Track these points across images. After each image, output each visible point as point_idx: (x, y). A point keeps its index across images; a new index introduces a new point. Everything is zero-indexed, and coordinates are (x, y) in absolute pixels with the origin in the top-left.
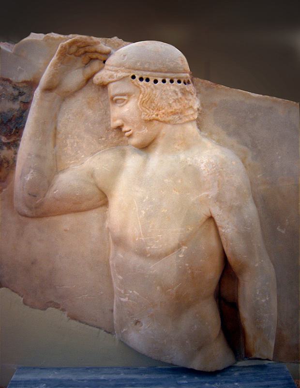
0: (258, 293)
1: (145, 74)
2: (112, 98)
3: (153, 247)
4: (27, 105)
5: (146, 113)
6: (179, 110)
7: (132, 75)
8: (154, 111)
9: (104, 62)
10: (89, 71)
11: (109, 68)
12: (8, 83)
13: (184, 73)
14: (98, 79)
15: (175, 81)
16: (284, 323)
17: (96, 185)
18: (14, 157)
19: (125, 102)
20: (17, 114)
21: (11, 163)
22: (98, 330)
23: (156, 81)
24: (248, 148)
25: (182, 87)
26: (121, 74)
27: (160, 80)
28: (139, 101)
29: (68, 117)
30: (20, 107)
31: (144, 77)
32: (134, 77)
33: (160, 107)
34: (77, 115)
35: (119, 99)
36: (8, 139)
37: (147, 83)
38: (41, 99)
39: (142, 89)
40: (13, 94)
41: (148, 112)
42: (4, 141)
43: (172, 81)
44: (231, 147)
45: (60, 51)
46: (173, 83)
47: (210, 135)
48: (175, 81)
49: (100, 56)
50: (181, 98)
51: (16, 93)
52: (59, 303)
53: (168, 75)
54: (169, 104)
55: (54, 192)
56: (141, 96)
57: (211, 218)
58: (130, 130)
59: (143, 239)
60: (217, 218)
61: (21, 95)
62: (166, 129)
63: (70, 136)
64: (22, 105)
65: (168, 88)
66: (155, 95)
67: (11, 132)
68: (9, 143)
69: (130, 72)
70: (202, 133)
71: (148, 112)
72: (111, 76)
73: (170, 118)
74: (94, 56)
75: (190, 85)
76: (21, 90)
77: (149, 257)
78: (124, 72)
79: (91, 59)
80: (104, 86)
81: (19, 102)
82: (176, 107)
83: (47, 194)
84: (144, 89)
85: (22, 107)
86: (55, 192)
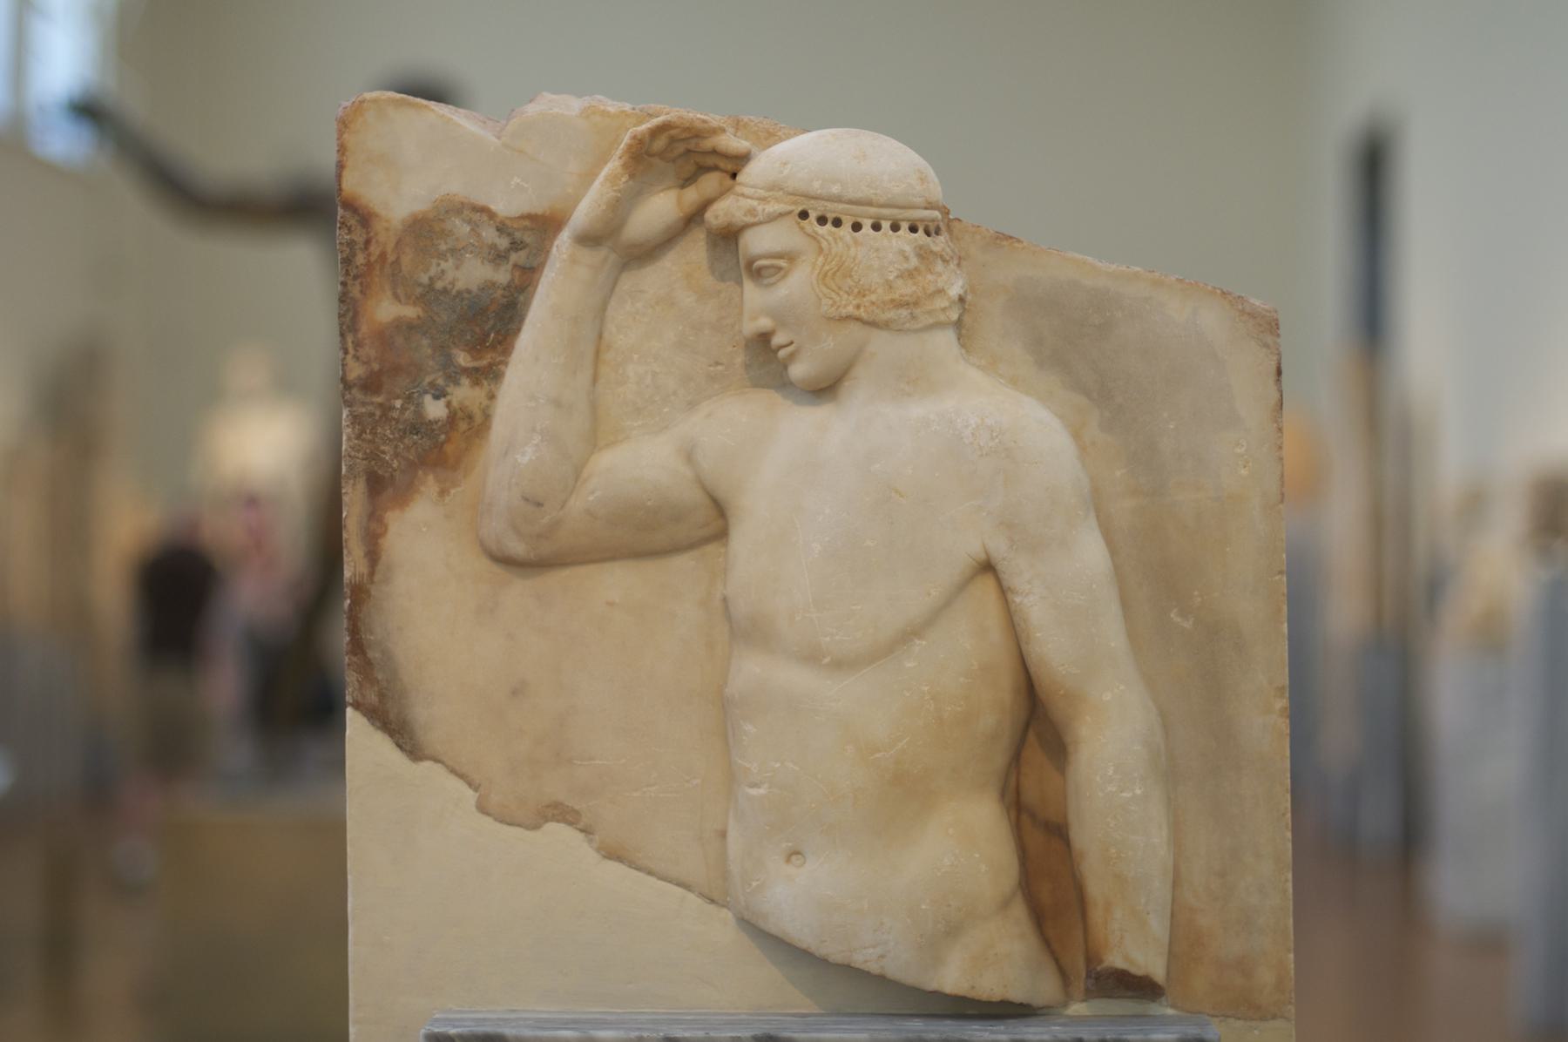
0: (1111, 772)
1: (832, 210)
2: (750, 264)
4: (528, 277)
9: (734, 176)
10: (692, 195)
11: (747, 191)
14: (716, 217)
15: (905, 226)
21: (478, 419)
23: (857, 227)
26: (773, 207)
27: (867, 224)
32: (804, 215)
36: (474, 359)
38: (573, 261)
39: (824, 244)
43: (895, 228)
45: (630, 147)
48: (905, 226)
50: (916, 269)
51: (503, 243)
52: (577, 807)
56: (821, 259)
57: (988, 567)
61: (517, 250)
62: (880, 343)
64: (517, 274)
67: (484, 341)
68: (477, 370)
69: (795, 203)
72: (751, 212)
73: (891, 314)
74: (710, 161)
75: (941, 238)
76: (518, 235)
79: (703, 169)
80: (728, 237)
81: (509, 267)
82: (905, 289)
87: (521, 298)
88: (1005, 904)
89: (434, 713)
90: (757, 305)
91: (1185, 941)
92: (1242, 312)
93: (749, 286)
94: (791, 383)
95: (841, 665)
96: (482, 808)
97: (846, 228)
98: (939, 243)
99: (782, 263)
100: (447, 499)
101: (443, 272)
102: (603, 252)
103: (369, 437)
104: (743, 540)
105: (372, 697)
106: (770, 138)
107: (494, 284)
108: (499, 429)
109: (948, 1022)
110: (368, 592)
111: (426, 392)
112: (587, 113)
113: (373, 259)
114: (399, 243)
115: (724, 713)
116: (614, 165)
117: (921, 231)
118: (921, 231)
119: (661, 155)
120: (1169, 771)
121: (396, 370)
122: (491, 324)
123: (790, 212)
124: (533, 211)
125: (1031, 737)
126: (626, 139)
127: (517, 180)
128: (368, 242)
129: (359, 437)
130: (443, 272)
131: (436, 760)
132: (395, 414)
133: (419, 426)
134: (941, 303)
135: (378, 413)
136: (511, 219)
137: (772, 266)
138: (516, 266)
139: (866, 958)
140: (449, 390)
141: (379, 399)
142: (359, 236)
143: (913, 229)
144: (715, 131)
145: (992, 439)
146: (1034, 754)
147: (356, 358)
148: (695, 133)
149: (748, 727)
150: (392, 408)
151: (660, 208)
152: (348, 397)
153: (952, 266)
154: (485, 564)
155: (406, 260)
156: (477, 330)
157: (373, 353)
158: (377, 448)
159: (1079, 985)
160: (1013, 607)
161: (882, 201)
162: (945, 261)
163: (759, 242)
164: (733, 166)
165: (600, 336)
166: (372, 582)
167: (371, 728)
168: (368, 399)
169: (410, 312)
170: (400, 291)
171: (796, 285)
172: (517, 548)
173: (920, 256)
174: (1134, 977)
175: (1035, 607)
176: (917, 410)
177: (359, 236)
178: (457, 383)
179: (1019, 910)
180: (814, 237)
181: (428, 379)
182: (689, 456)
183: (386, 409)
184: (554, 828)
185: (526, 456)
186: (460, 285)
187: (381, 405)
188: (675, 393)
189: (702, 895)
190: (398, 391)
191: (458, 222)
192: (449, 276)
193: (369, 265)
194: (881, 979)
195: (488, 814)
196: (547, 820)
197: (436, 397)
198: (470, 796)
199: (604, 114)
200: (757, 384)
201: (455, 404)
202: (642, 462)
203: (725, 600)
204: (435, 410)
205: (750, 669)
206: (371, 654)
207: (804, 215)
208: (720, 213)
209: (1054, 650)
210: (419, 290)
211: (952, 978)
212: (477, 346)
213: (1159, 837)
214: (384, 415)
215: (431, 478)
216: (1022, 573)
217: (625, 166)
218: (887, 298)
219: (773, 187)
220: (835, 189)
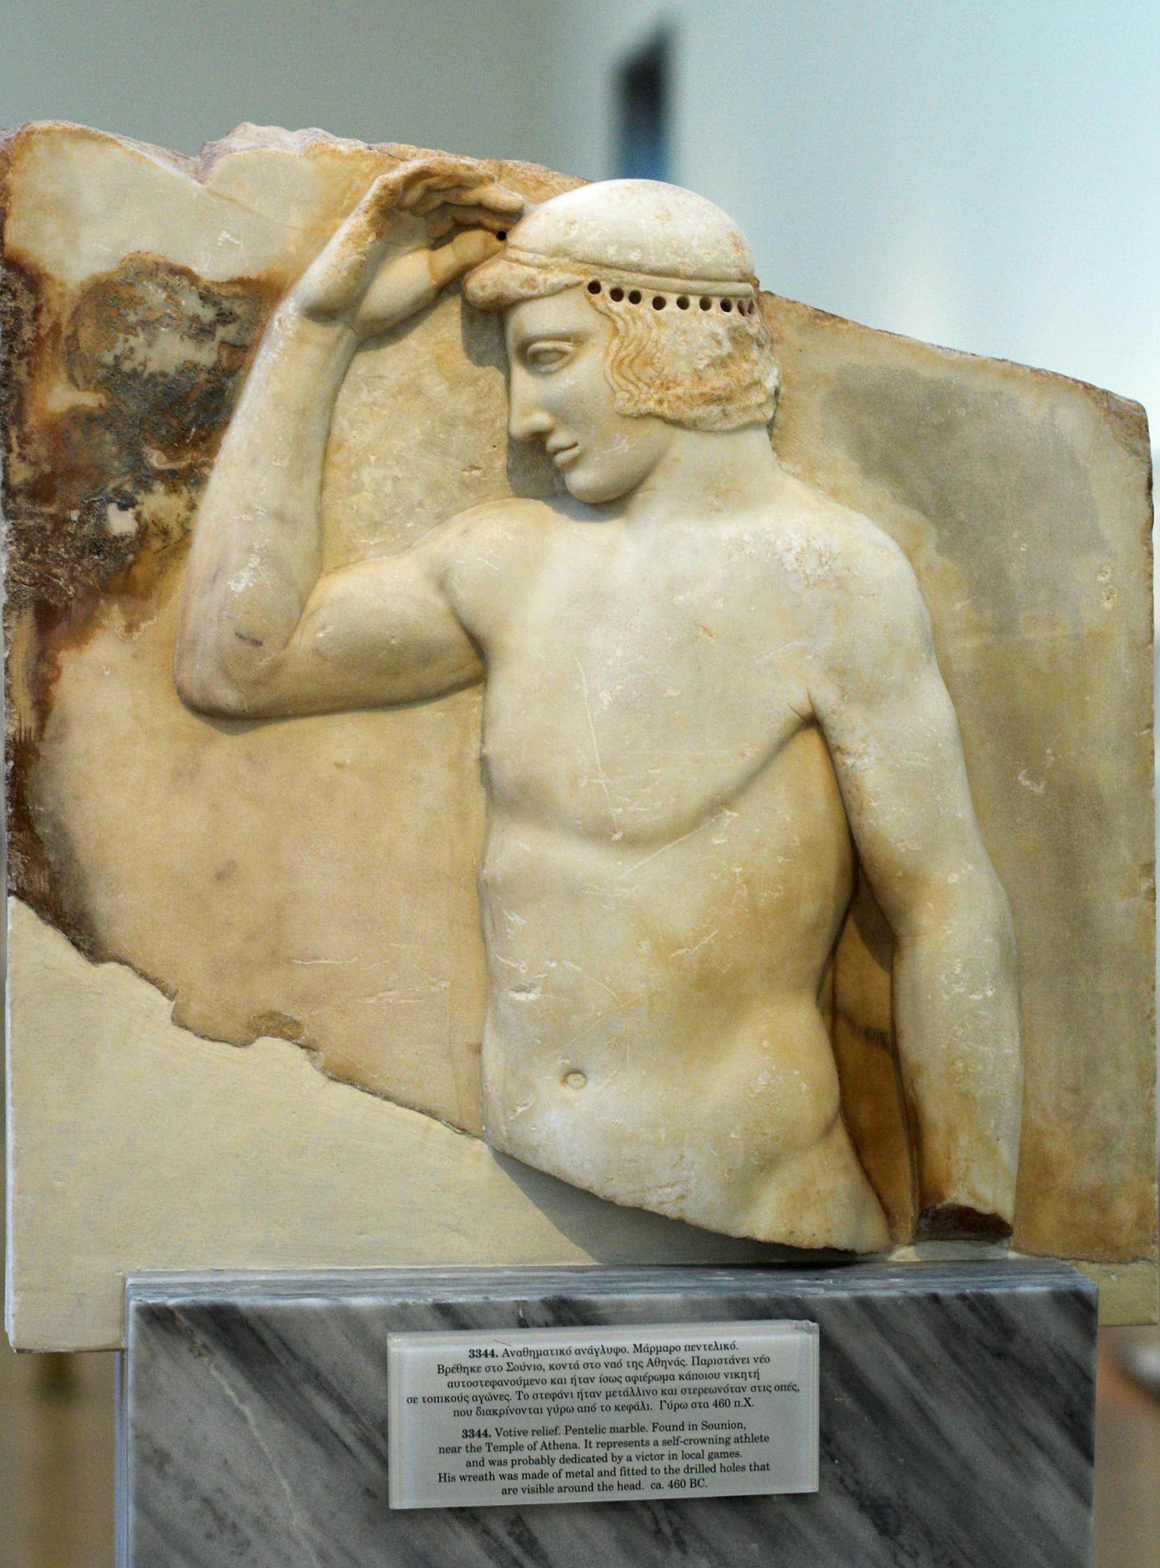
0: (958, 970)
1: (630, 282)
3: (631, 809)
4: (237, 358)
5: (627, 396)
6: (724, 389)
7: (591, 279)
8: (652, 391)
9: (502, 236)
10: (447, 258)
12: (185, 282)
13: (740, 281)
14: (483, 288)
15: (716, 302)
16: (1050, 1108)
18: (188, 519)
19: (566, 359)
20: (208, 381)
21: (176, 534)
23: (659, 303)
24: (925, 512)
25: (735, 323)
26: (557, 278)
27: (672, 299)
28: (611, 358)
29: (371, 399)
30: (220, 361)
31: (627, 290)
32: (594, 287)
33: (670, 378)
34: (400, 392)
35: (547, 351)
36: (171, 459)
38: (301, 339)
39: (620, 324)
40: (198, 317)
41: (636, 392)
42: (156, 465)
43: (705, 305)
44: (875, 513)
45: (379, 198)
46: (709, 312)
47: (809, 473)
48: (716, 302)
50: (730, 356)
51: (208, 314)
52: (298, 1018)
53: (695, 285)
54: (696, 370)
55: (317, 632)
56: (616, 342)
57: (812, 722)
58: (575, 445)
59: (602, 782)
60: (829, 721)
61: (225, 323)
62: (684, 444)
63: (373, 458)
64: (225, 354)
65: (695, 324)
66: (657, 343)
67: (184, 437)
68: (173, 473)
69: (585, 273)
70: (785, 465)
71: (636, 392)
72: (530, 282)
73: (700, 412)
74: (472, 217)
76: (226, 304)
77: (618, 842)
78: (568, 271)
79: (461, 227)
81: (215, 344)
82: (717, 381)
83: (296, 640)
84: (626, 324)
85: (224, 361)
86: (321, 635)
87: (230, 384)
88: (828, 1131)
89: (123, 899)
90: (531, 398)
91: (1035, 1172)
92: (1108, 411)
93: (519, 374)
94: (566, 493)
95: (638, 841)
96: (179, 1021)
97: (647, 304)
98: (754, 324)
99: (566, 346)
100: (136, 635)
101: (132, 350)
102: (338, 329)
103: (38, 557)
104: (509, 688)
105: (42, 884)
106: (542, 191)
107: (195, 366)
108: (203, 549)
109: (761, 1275)
110: (36, 752)
111: (110, 501)
112: (310, 153)
113: (43, 332)
114: (76, 313)
115: (484, 900)
116: (355, 222)
117: (735, 310)
118: (735, 310)
119: (413, 209)
120: (1017, 967)
121: (72, 473)
122: (193, 415)
123: (578, 284)
124: (245, 276)
125: (851, 926)
126: (374, 189)
127: (225, 235)
128: (37, 311)
129: (25, 557)
130: (132, 350)
131: (122, 962)
132: (71, 529)
133: (100, 543)
134: (757, 397)
135: (49, 526)
136: (217, 284)
137: (555, 351)
138: (223, 343)
140: (139, 498)
141: (51, 510)
142: (26, 304)
144: (481, 181)
145: (821, 565)
146: (855, 948)
147: (22, 457)
148: (459, 183)
149: (516, 919)
150: (68, 521)
151: (410, 272)
152: (11, 506)
153: (767, 352)
154: (182, 717)
155: (86, 335)
156: (174, 422)
157: (43, 451)
158: (49, 572)
159: (907, 1227)
160: (842, 771)
161: (690, 271)
162: (760, 346)
163: (537, 320)
164: (502, 223)
165: (329, 433)
166: (41, 739)
167: (40, 923)
168: (37, 509)
169: (90, 400)
170: (78, 373)
172: (228, 697)
173: (733, 339)
174: (981, 1215)
175: (869, 770)
176: (730, 528)
177: (26, 304)
178: (149, 490)
179: (840, 1138)
180: (607, 315)
182: (442, 583)
183: (60, 522)
185: (241, 583)
186: (153, 367)
187: (52, 516)
188: (421, 504)
189: (450, 1124)
190: (74, 499)
191: (151, 287)
192: (140, 356)
193: (38, 339)
194: (680, 1225)
195: (187, 1029)
196: (259, 1034)
197: (123, 507)
198: (165, 1006)
199: (335, 153)
200: (521, 492)
201: (146, 515)
202: (380, 590)
203: (483, 761)
204: (121, 523)
205: (518, 846)
206: (39, 830)
207: (594, 287)
208: (487, 281)
209: (891, 822)
210: (101, 373)
211: (765, 1221)
212: (175, 444)
213: (1010, 1047)
214: (57, 529)
215: (116, 608)
217: (372, 222)
218: (696, 392)
219: (559, 252)
220: (634, 257)
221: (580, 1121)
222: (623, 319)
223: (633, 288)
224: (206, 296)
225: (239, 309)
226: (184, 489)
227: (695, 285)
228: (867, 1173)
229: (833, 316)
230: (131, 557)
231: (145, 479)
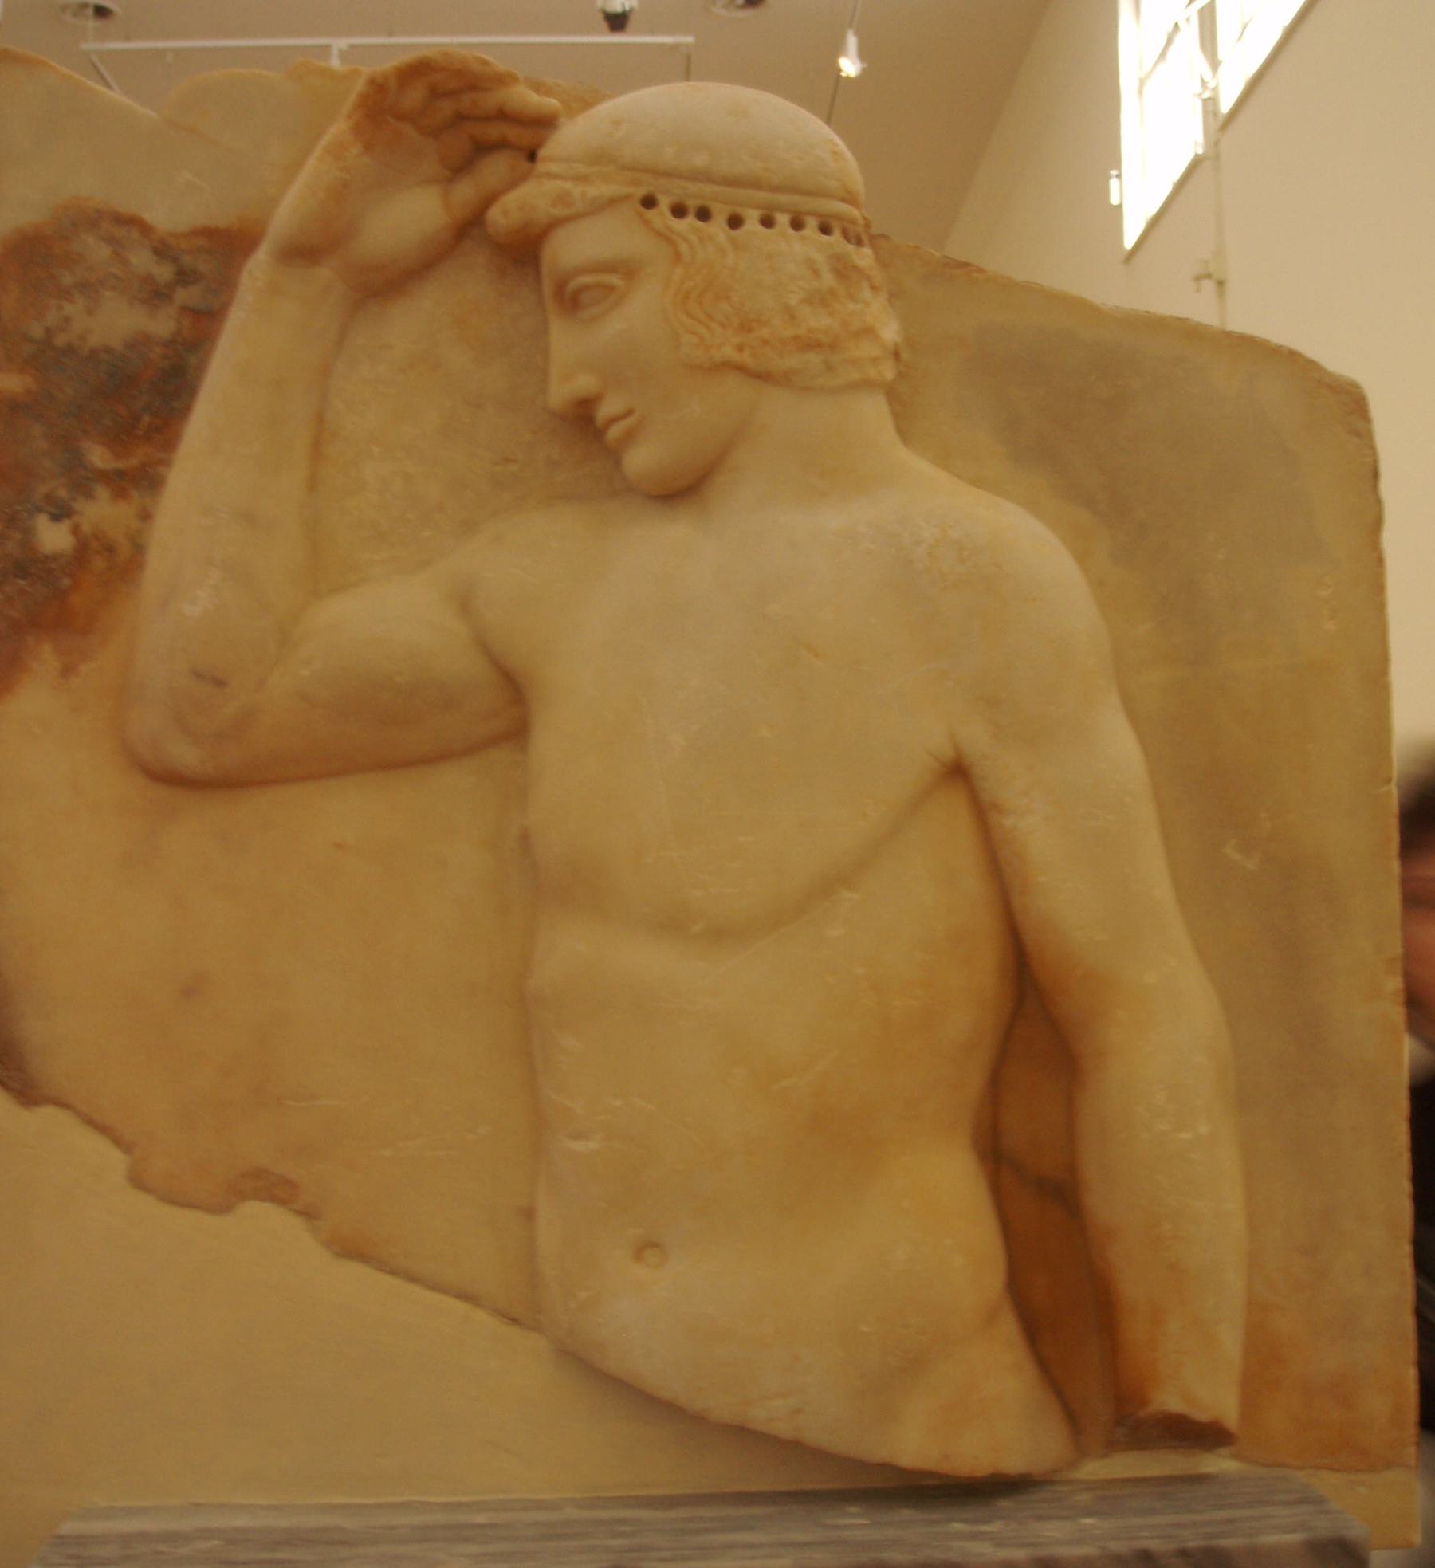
1: (695, 193)
4: (203, 324)
9: (532, 156)
10: (465, 191)
11: (554, 168)
12: (135, 234)
13: (843, 200)
14: (506, 213)
17: (484, 646)
22: (460, 1306)
23: (735, 222)
26: (600, 190)
27: (752, 217)
31: (692, 204)
32: (649, 202)
35: (587, 287)
37: (700, 224)
39: (684, 248)
43: (797, 225)
45: (364, 99)
48: (812, 223)
49: (512, 133)
53: (782, 198)
56: (679, 271)
57: (957, 772)
58: (629, 412)
68: (121, 474)
72: (563, 199)
73: (792, 361)
74: (494, 131)
76: (187, 260)
79: (483, 148)
82: (817, 321)
87: (193, 360)
90: (573, 357)
91: (1263, 1363)
95: (721, 935)
96: (138, 1181)
97: (717, 228)
99: (614, 280)
104: (550, 740)
109: (907, 1514)
111: (40, 510)
122: (146, 401)
133: (30, 565)
137: (599, 286)
138: (185, 310)
139: (771, 1413)
143: (825, 230)
162: (873, 288)
163: (574, 249)
171: (637, 316)
172: (186, 756)
175: (1037, 833)
178: (89, 495)
179: (1009, 1325)
181: (43, 489)
182: (464, 603)
184: (259, 1213)
186: (94, 341)
191: (91, 240)
196: (243, 1196)
197: (55, 518)
198: (117, 1160)
201: (86, 528)
204: (53, 537)
205: (570, 948)
207: (649, 202)
209: (1069, 902)
211: (912, 1445)
212: (121, 437)
216: (1011, 778)
217: (357, 130)
220: (700, 161)
221: (658, 1308)
222: (686, 240)
223: (699, 202)
224: (162, 250)
225: (203, 265)
226: (135, 494)
227: (782, 198)
228: (1043, 1364)
229: (967, 265)
230: (66, 582)
231: (83, 481)
